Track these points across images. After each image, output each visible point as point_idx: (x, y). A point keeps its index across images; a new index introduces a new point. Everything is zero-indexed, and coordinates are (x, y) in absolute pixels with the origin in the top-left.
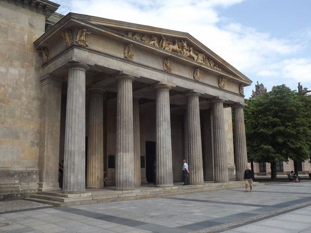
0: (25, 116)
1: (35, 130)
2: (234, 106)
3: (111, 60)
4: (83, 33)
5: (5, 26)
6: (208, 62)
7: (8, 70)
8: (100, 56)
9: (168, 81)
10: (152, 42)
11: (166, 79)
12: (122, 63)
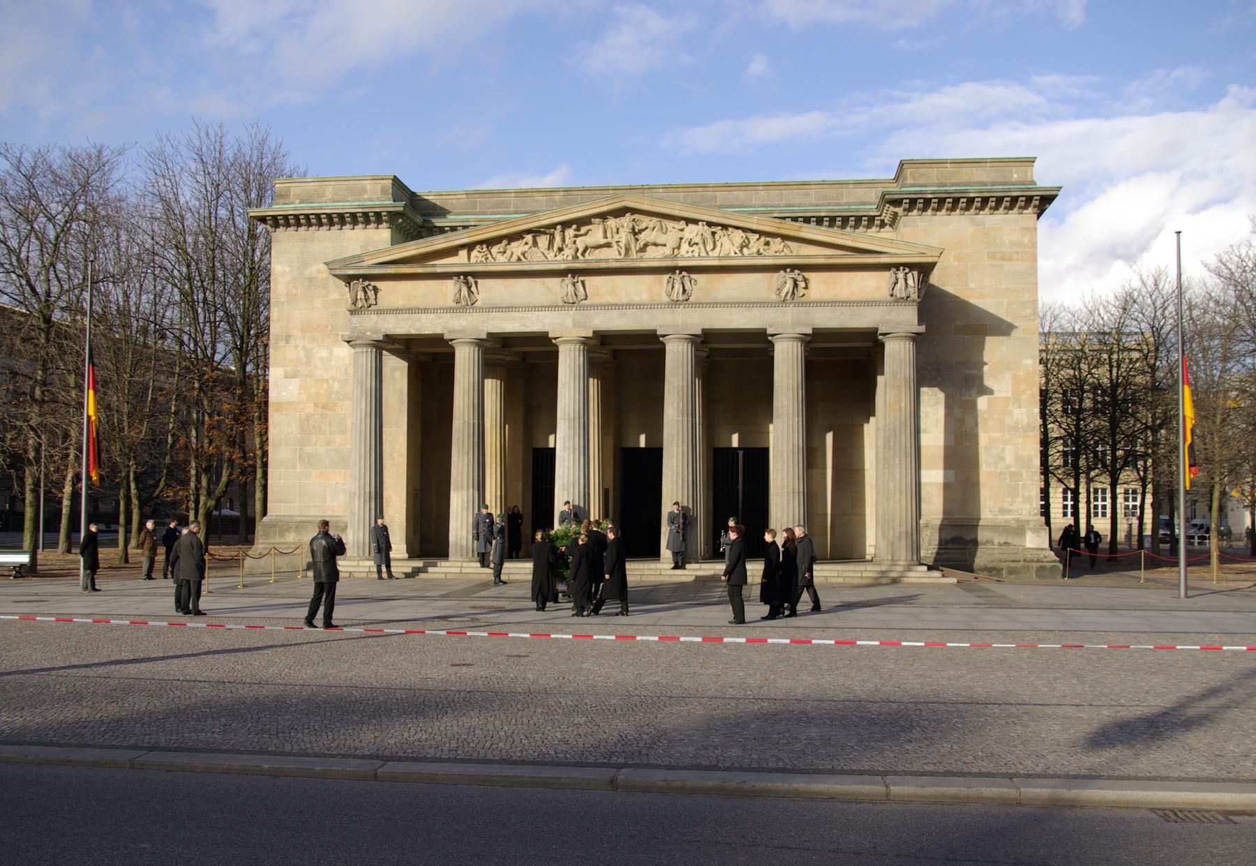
3: (424, 316)
5: (324, 276)
6: (725, 240)
7: (331, 352)
8: (400, 316)
9: (574, 325)
11: (569, 323)
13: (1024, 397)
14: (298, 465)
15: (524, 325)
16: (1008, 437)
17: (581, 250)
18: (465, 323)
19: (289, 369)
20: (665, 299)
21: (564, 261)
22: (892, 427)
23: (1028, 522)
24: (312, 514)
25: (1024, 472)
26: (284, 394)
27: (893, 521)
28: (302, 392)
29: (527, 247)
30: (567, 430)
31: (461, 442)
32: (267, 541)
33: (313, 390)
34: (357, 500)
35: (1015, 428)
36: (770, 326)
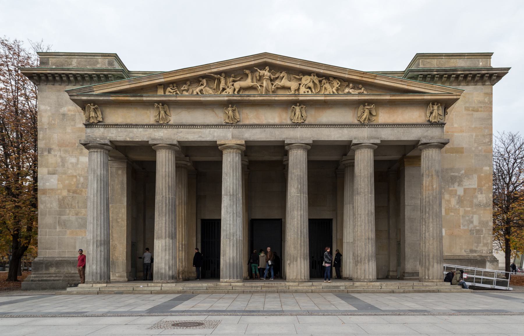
3: (135, 130)
5: (73, 113)
6: (327, 86)
9: (233, 138)
11: (229, 135)
12: (152, 130)
13: (484, 188)
15: (200, 137)
16: (475, 210)
17: (237, 90)
20: (289, 122)
21: (228, 96)
22: (427, 199)
23: (486, 257)
25: (484, 229)
27: (429, 255)
29: (203, 87)
30: (229, 201)
31: (160, 208)
34: (91, 245)
35: (479, 205)
36: (355, 138)
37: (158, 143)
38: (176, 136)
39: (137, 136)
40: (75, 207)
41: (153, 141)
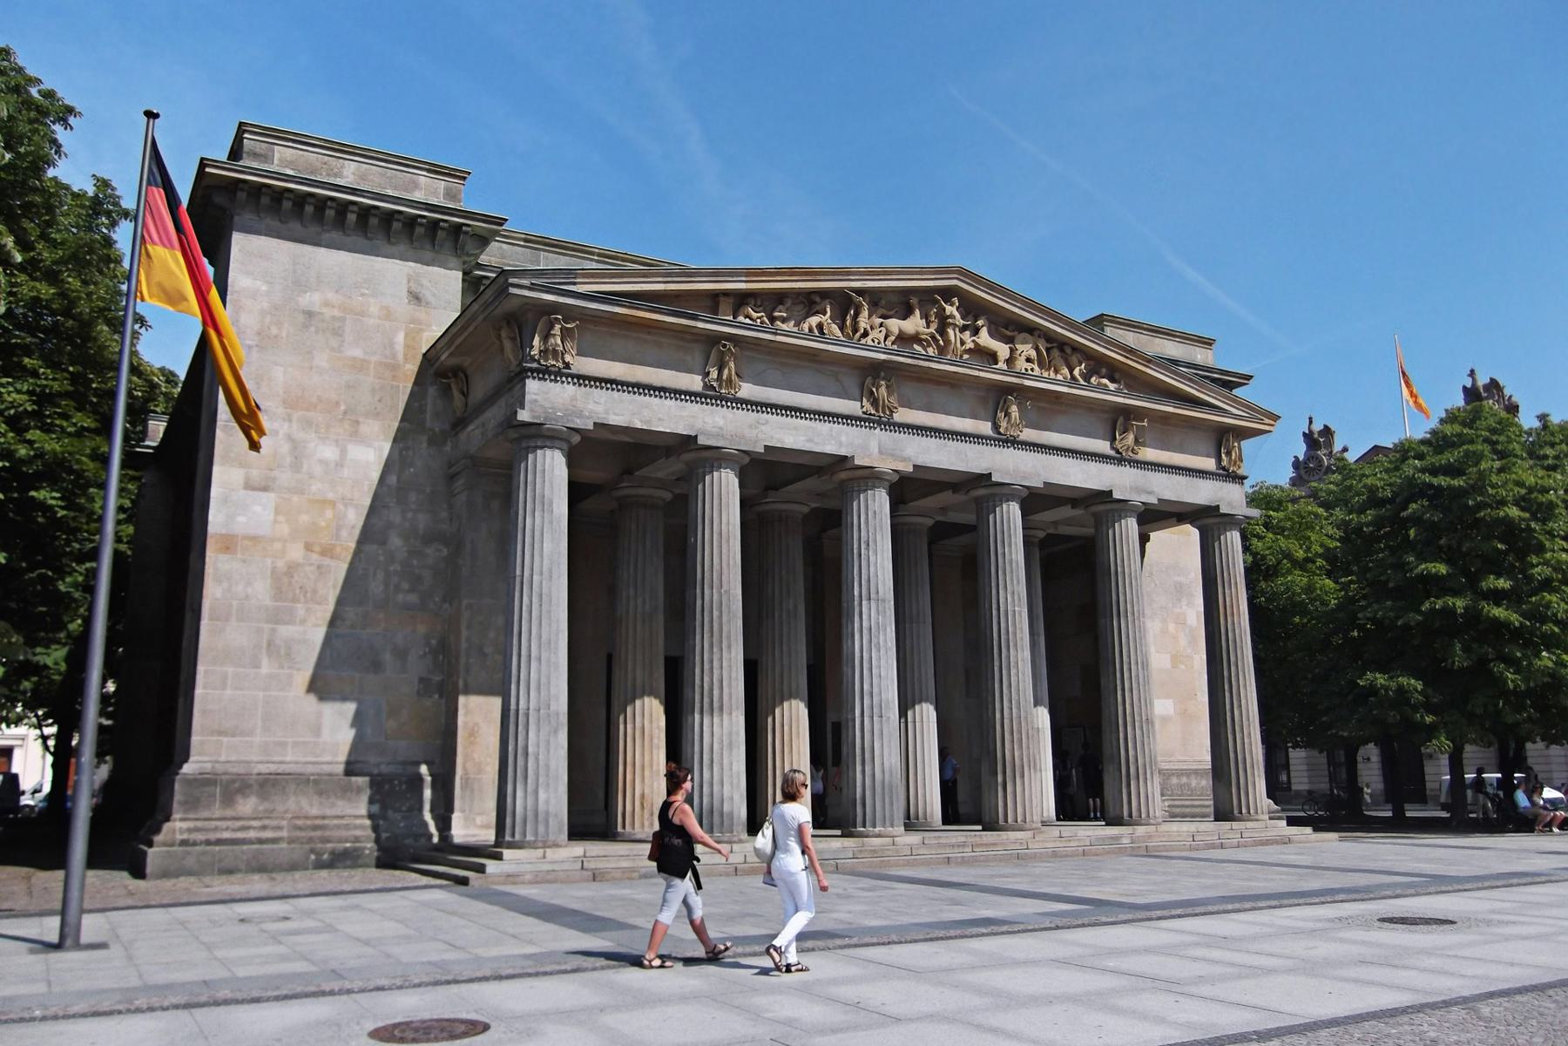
0: (400, 597)
1: (434, 642)
2: (1207, 520)
4: (552, 327)
5: (336, 313)
7: (343, 452)
9: (880, 452)
10: (814, 320)
11: (874, 447)
14: (265, 662)
15: (810, 440)
18: (721, 423)
19: (255, 473)
24: (288, 758)
26: (241, 519)
28: (281, 518)
32: (192, 816)
33: (304, 518)
37: (719, 445)
38: (755, 432)
39: (660, 419)
40: (327, 599)
41: (708, 439)
